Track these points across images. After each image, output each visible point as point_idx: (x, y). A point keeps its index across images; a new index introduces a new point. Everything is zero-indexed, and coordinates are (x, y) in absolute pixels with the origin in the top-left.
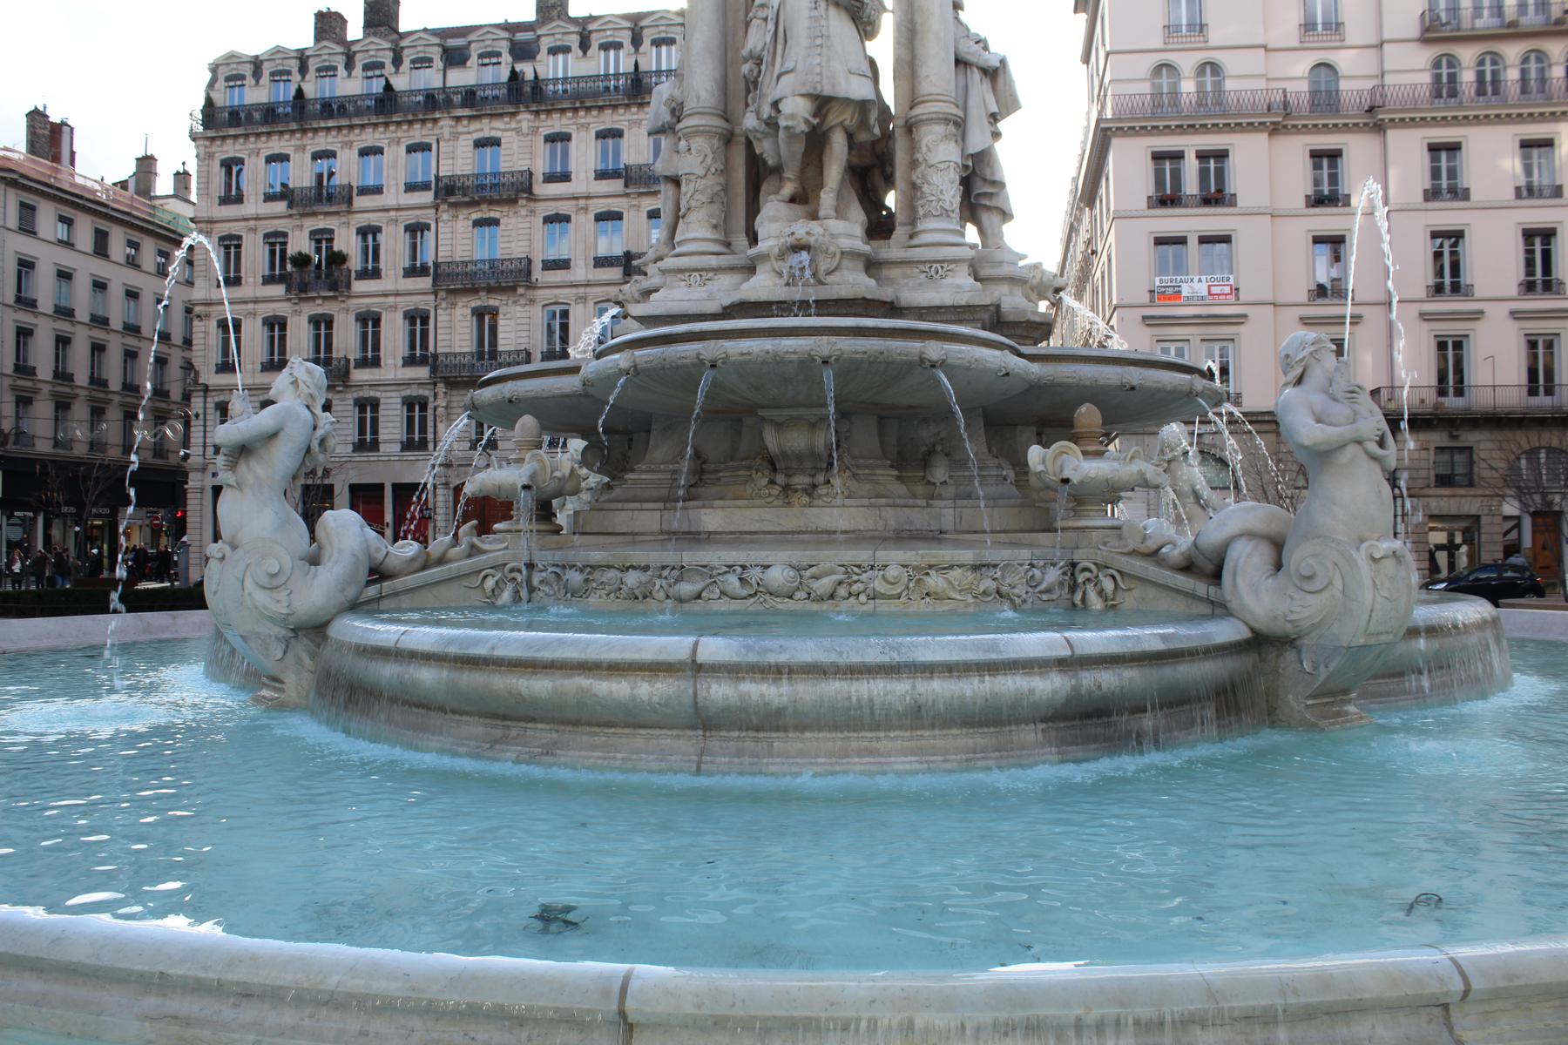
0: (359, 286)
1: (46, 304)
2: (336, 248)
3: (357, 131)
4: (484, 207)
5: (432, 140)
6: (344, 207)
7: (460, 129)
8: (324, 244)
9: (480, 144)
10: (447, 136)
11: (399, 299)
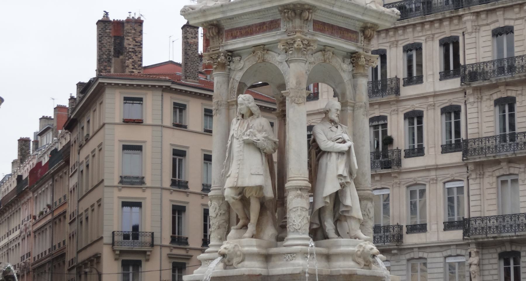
0: (409, 163)
1: (195, 186)
2: (389, 134)
3: (400, 32)
4: (502, 88)
5: (459, 34)
6: (393, 97)
7: (481, 23)
8: (380, 130)
9: (497, 33)
10: (470, 29)
11: (440, 172)
